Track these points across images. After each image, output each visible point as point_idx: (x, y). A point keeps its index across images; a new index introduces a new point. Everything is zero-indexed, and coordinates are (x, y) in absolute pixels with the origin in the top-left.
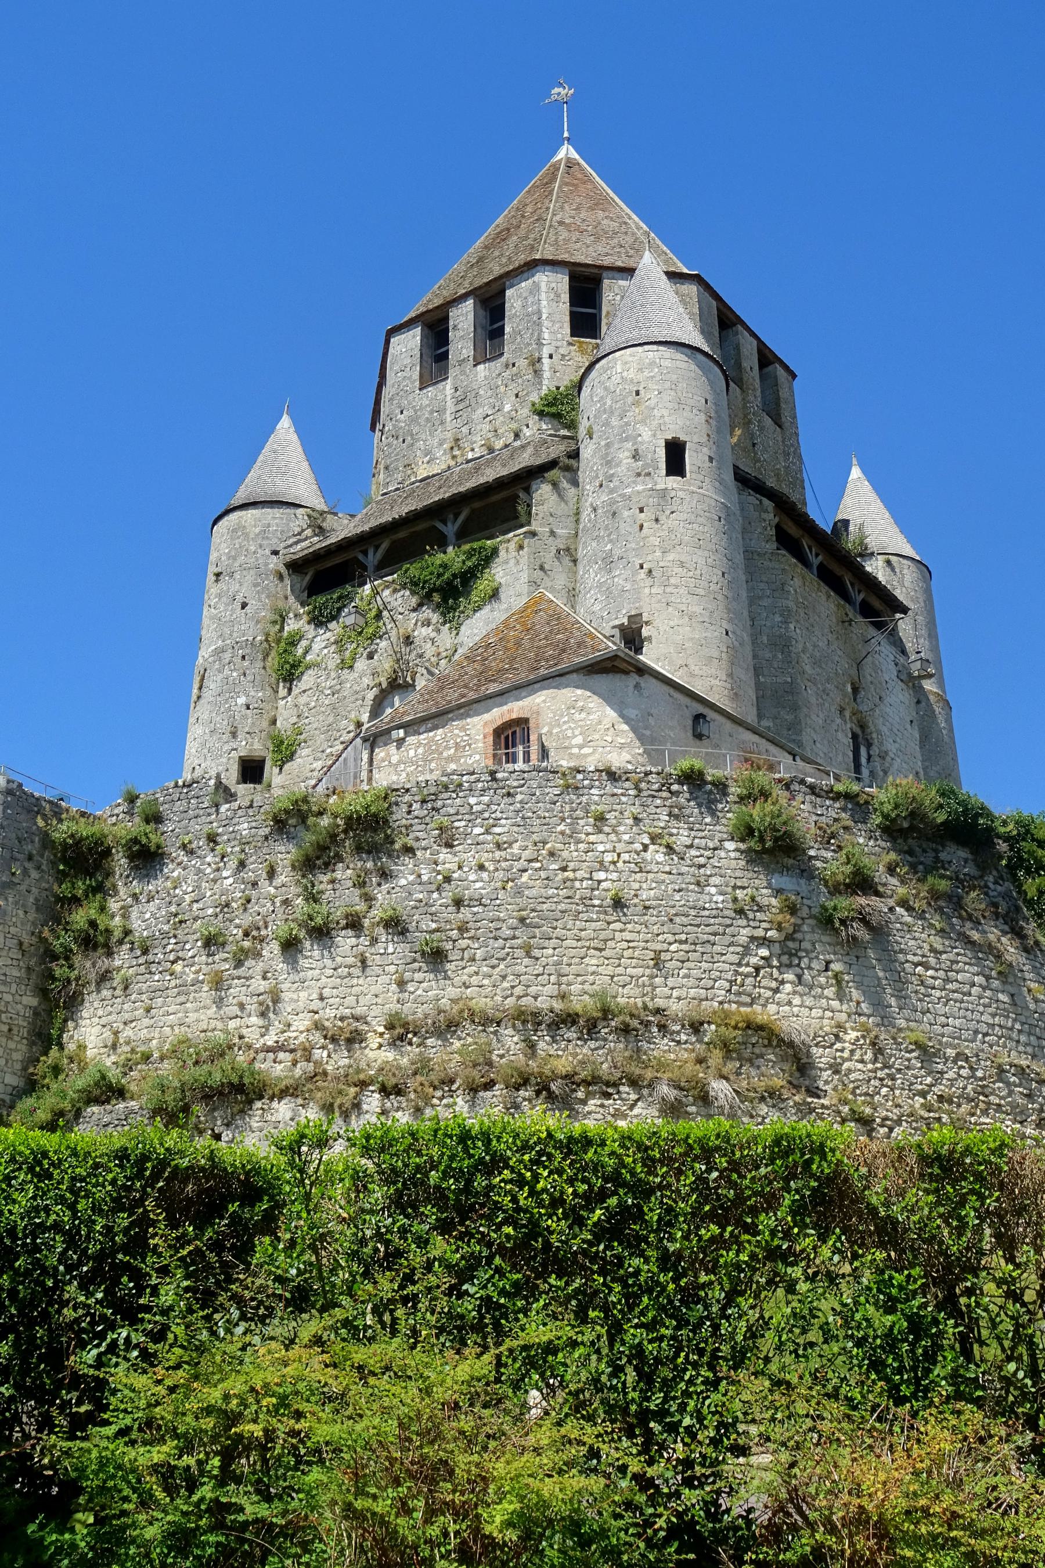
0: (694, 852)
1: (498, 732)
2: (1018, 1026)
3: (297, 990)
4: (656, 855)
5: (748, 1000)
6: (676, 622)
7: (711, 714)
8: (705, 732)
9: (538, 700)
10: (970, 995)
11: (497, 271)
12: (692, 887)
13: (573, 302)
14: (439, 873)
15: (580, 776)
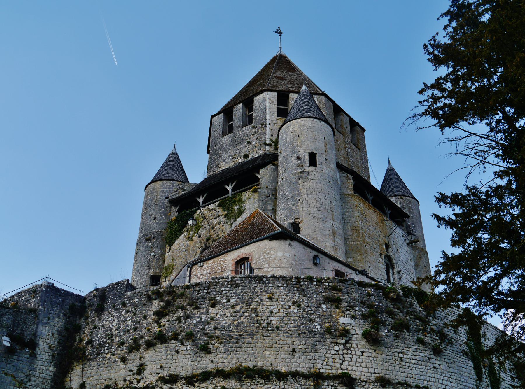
0: (309, 309)
2: (442, 377)
4: (294, 309)
5: (330, 368)
6: (313, 221)
7: (320, 255)
8: (318, 262)
9: (252, 251)
10: (421, 365)
11: (251, 94)
12: (308, 322)
13: (278, 104)
14: (209, 318)
15: (265, 279)
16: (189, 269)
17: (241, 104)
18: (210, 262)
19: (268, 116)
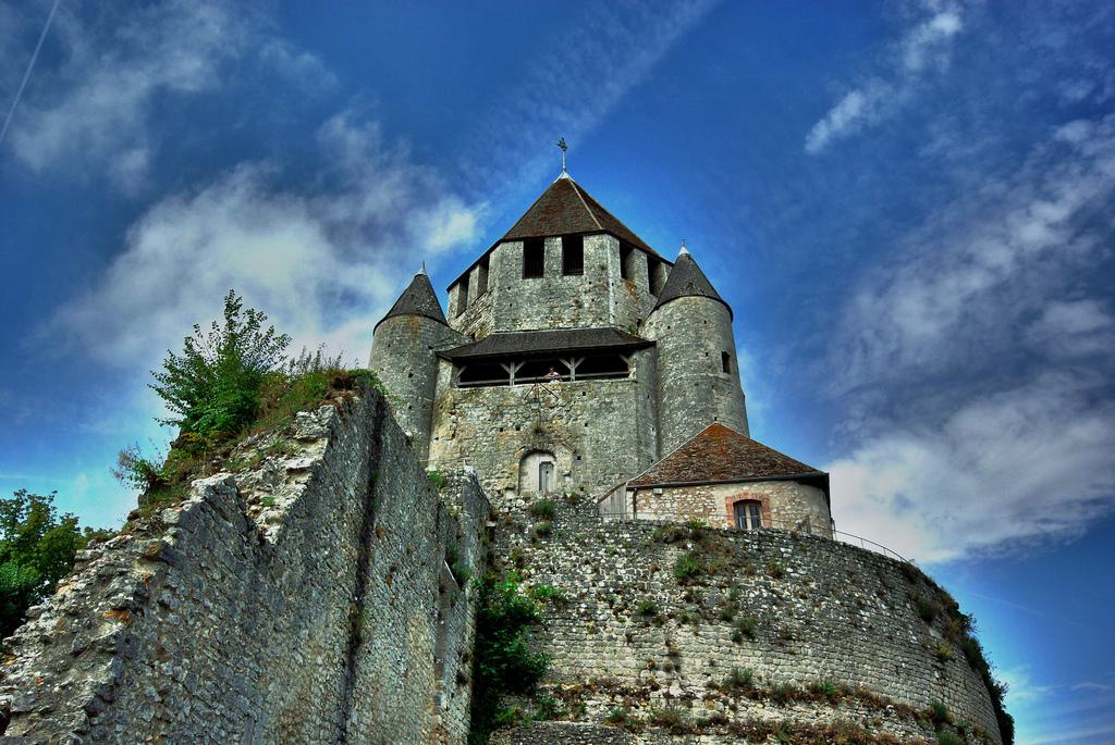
1: (735, 504)
3: (692, 657)
9: (767, 492)
16: (631, 494)
17: (559, 239)
18: (675, 492)
19: (610, 272)
